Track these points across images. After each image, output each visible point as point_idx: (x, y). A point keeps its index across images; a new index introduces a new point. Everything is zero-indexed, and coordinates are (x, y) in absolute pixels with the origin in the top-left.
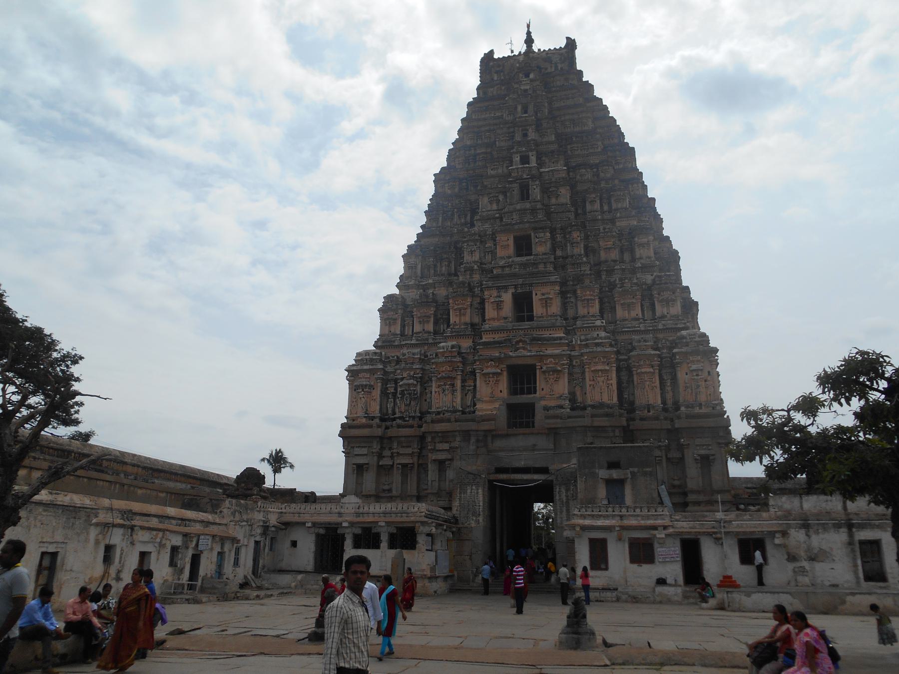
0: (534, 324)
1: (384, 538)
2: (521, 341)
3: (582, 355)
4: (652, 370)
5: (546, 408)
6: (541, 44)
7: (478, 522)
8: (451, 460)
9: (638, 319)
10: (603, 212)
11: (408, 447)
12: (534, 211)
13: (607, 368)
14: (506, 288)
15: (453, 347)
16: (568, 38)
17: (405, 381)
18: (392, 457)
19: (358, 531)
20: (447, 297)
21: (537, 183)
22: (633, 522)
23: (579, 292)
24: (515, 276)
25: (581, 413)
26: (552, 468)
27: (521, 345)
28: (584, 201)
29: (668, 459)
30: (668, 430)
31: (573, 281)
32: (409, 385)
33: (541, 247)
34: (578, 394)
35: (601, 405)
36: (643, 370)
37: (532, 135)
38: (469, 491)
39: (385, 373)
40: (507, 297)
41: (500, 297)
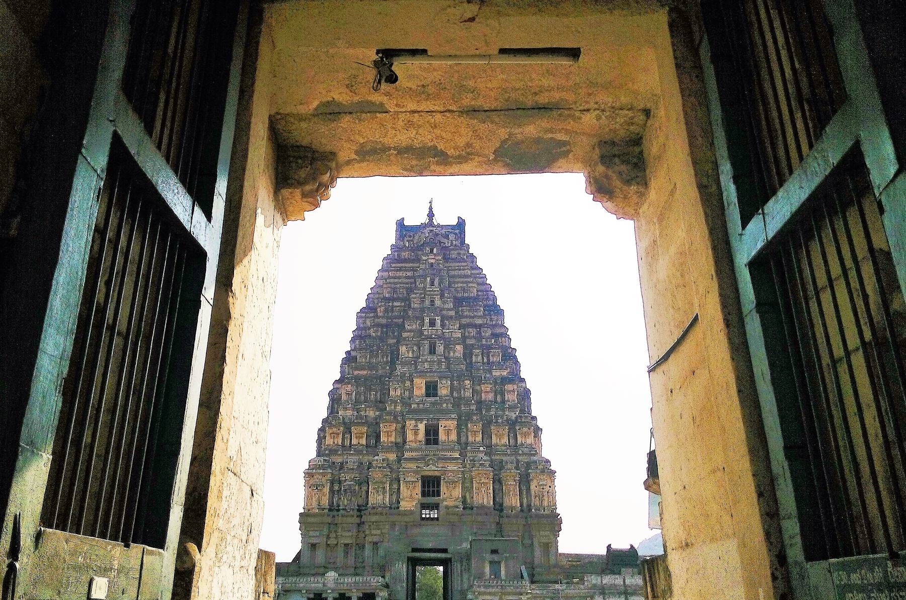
0: (440, 447)
5: (447, 507)
6: (439, 220)
10: (483, 363)
12: (439, 362)
14: (421, 420)
15: (383, 460)
16: (459, 218)
17: (348, 483)
18: (336, 538)
20: (376, 419)
22: (509, 590)
24: (425, 411)
26: (451, 549)
28: (471, 354)
32: (349, 485)
33: (443, 391)
34: (468, 497)
35: (482, 507)
37: (438, 303)
40: (422, 427)
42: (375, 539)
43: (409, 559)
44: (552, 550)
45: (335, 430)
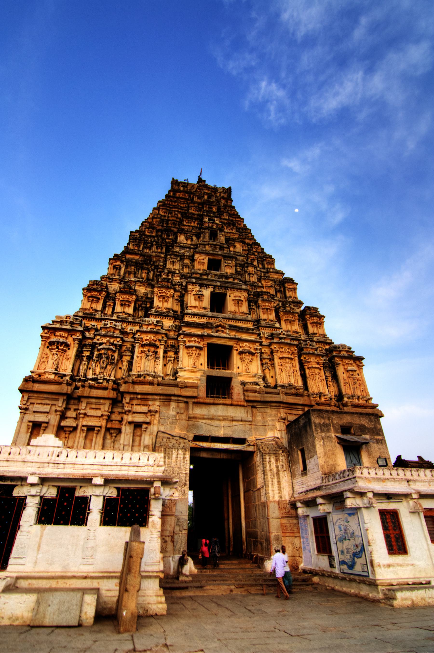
1: (96, 506)
2: (220, 326)
3: (271, 344)
4: (317, 366)
5: (243, 384)
8: (148, 423)
9: (297, 333)
11: (97, 409)
13: (292, 357)
14: (206, 286)
18: (76, 419)
19: (51, 492)
21: (223, 233)
23: (260, 302)
25: (275, 391)
26: (251, 438)
27: (220, 329)
31: (253, 295)
35: (290, 386)
36: (314, 366)
38: (174, 456)
39: (85, 338)
40: (207, 293)
41: (201, 291)
42: (139, 419)
43: (193, 450)
45: (95, 293)
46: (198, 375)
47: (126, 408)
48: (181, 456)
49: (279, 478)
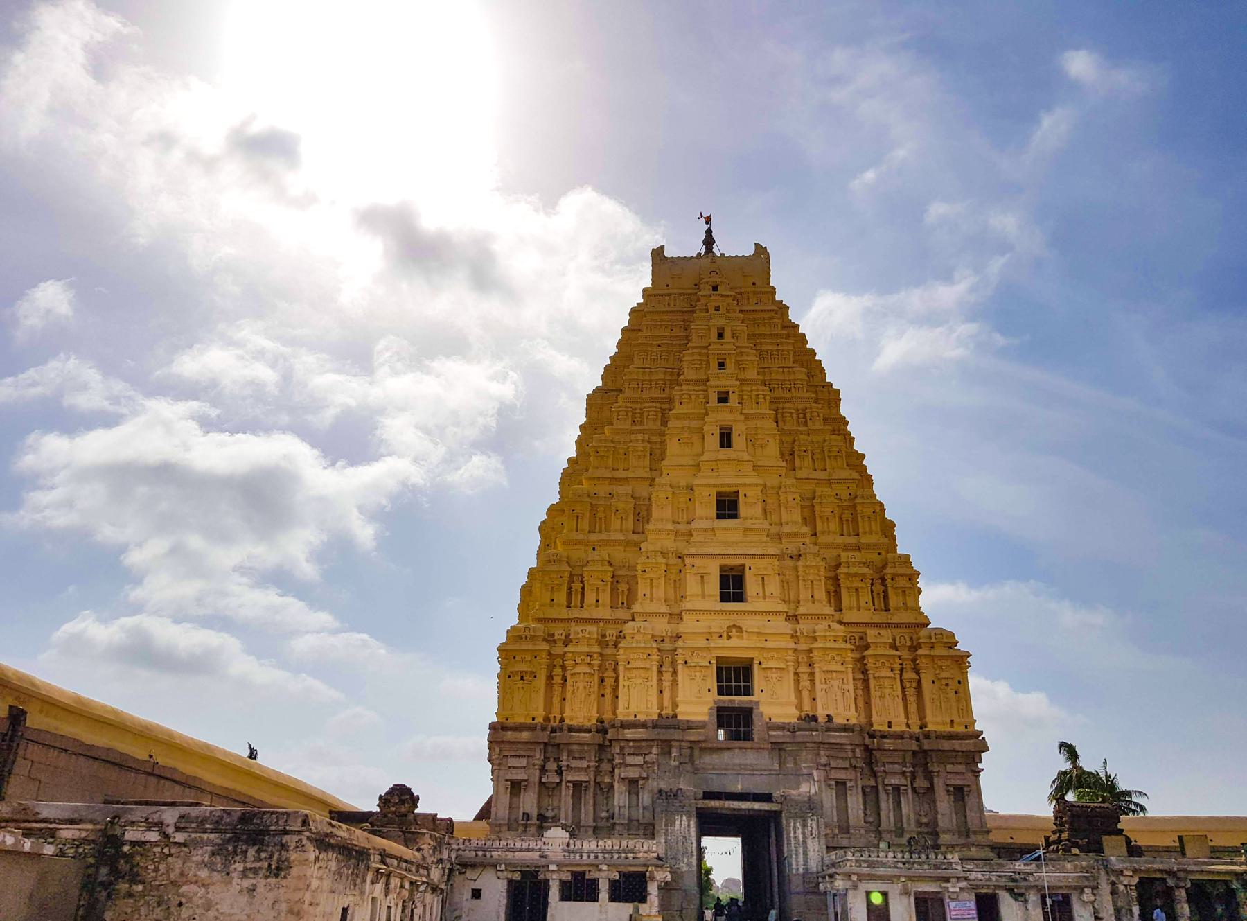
1: (604, 887)
2: (734, 626)
7: (689, 864)
8: (646, 779)
11: (581, 758)
16: (756, 244)
18: (559, 772)
26: (776, 794)
29: (914, 789)
30: (914, 752)
36: (883, 675)
38: (678, 823)
42: (633, 773)
44: (970, 801)
46: (705, 709)
47: (617, 761)
48: (685, 823)
49: (805, 847)
